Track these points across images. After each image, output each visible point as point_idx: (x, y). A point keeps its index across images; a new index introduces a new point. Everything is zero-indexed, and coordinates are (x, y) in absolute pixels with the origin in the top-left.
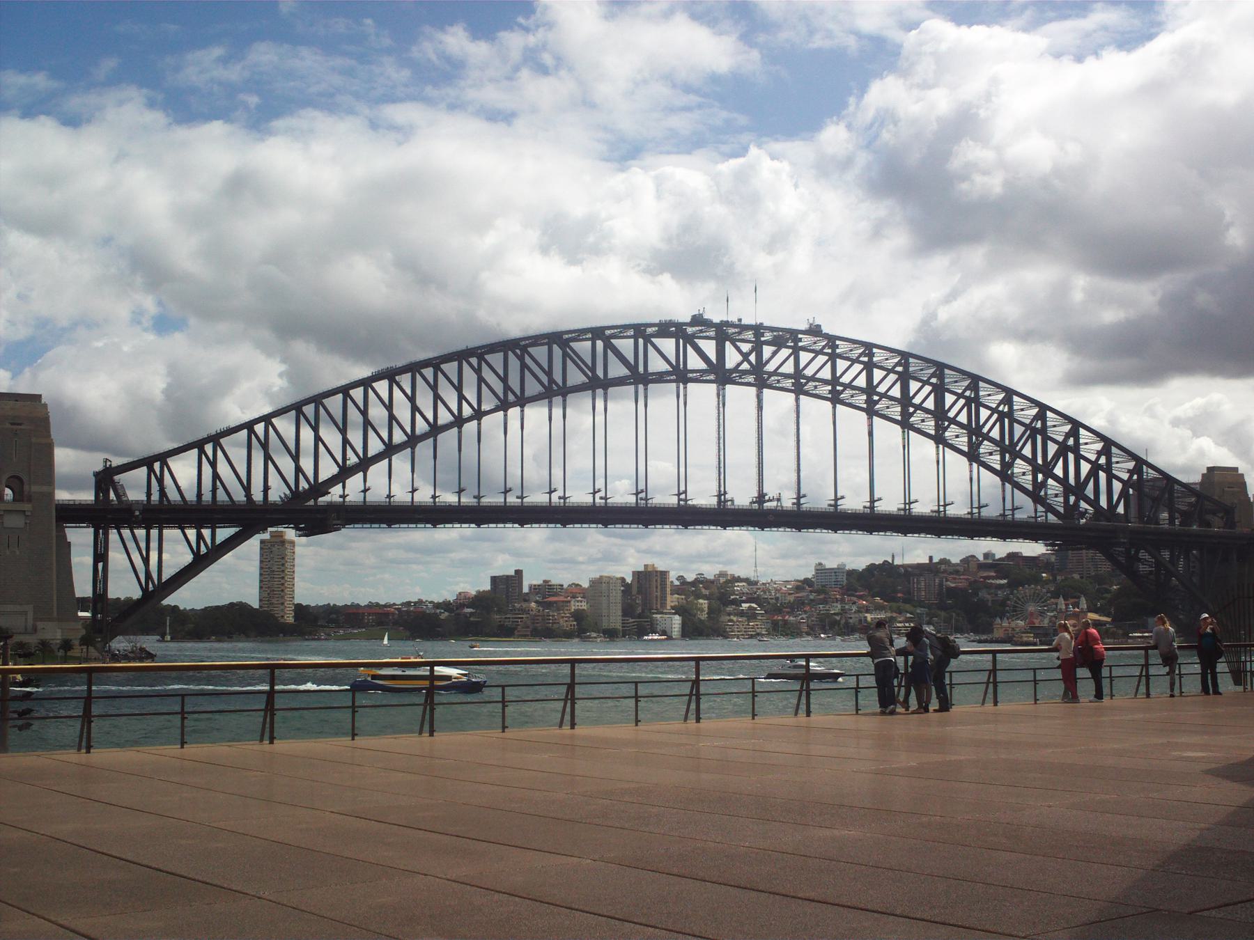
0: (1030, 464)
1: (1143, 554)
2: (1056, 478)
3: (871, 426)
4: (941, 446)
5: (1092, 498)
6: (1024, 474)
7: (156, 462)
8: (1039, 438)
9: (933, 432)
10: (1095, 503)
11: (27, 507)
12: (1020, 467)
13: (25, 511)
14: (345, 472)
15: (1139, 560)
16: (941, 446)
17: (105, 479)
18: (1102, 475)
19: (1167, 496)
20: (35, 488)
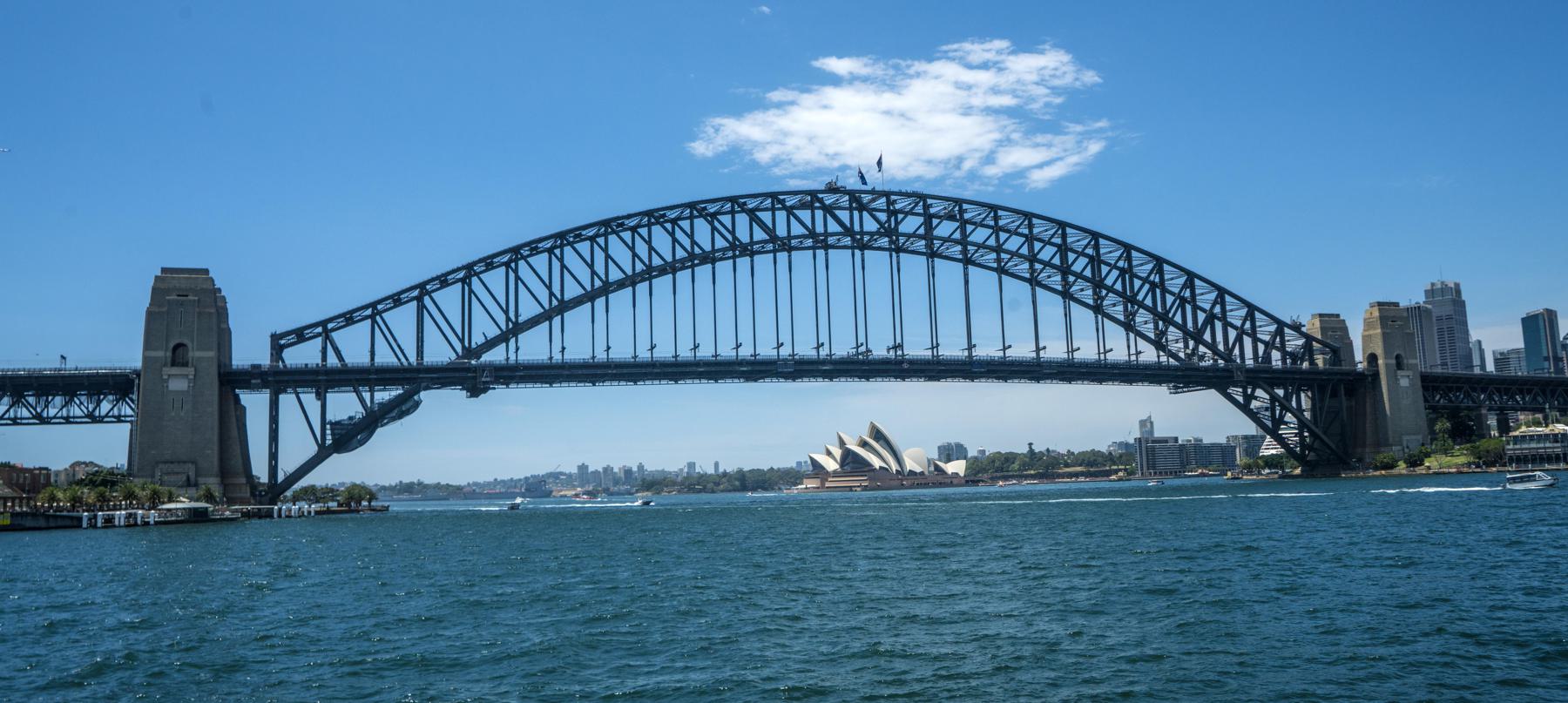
0: (1152, 313)
1: (1259, 393)
2: (1176, 325)
3: (966, 275)
4: (1100, 317)
5: (1210, 341)
6: (1146, 323)
7: (325, 329)
8: (1158, 291)
9: (1091, 302)
10: (1212, 346)
11: (190, 371)
12: (1142, 317)
13: (187, 375)
14: (503, 338)
15: (1256, 398)
16: (1100, 317)
17: (278, 345)
18: (1218, 325)
19: (1278, 340)
20: (198, 354)
